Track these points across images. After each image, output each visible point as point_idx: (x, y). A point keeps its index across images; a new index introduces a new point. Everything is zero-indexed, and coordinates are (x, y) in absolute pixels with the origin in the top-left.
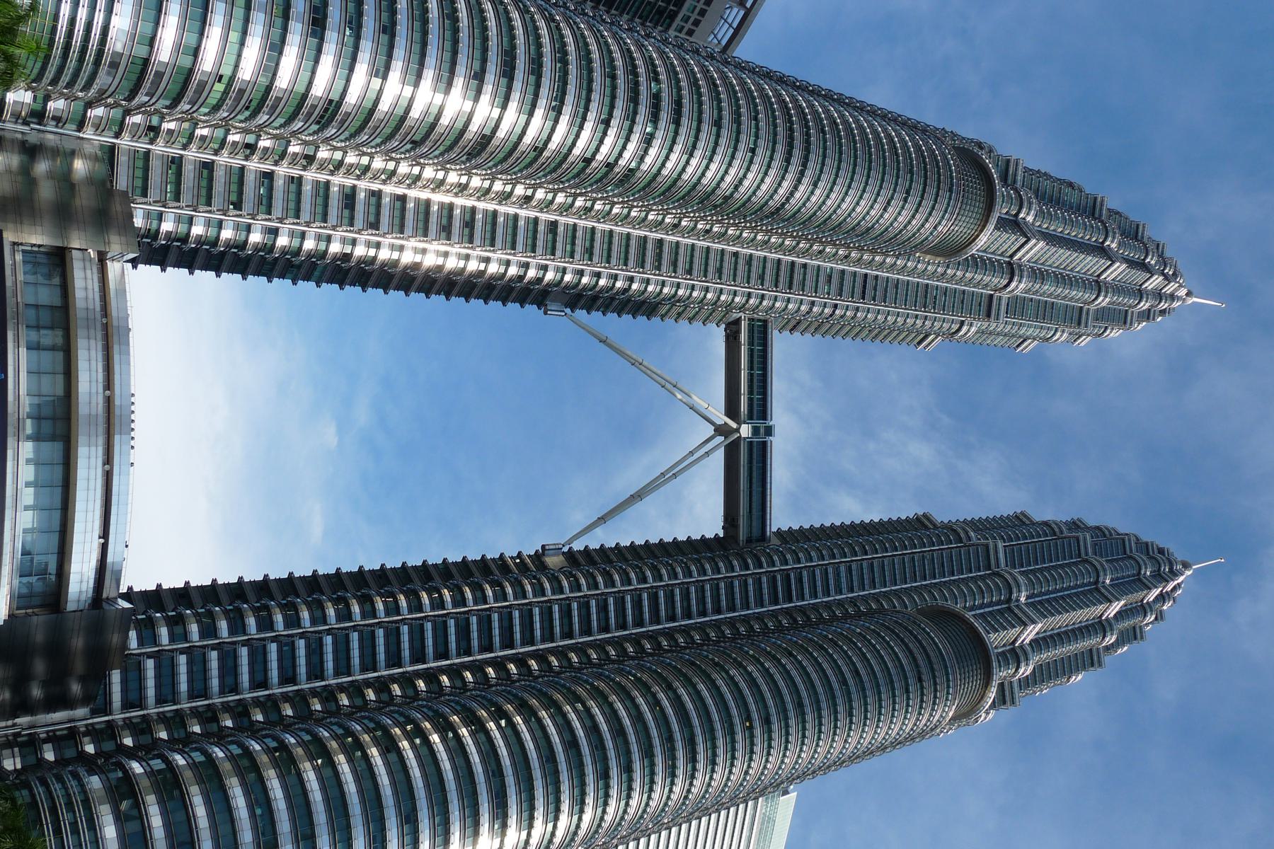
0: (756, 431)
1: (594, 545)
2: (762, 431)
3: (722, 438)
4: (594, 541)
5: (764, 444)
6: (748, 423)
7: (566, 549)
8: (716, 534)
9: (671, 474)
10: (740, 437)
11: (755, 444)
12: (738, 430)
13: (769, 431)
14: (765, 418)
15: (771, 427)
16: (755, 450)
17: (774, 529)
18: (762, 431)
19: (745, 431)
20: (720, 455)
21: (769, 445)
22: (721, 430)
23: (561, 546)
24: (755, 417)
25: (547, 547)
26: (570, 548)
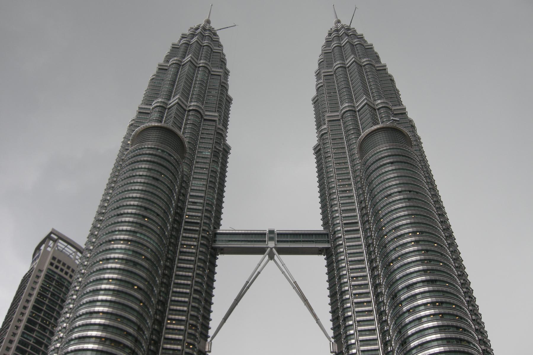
0: (271, 239)
1: (331, 325)
2: (271, 235)
3: (275, 256)
4: (328, 325)
5: (278, 234)
6: (268, 243)
7: (333, 340)
8: (325, 259)
9: (294, 284)
10: (275, 248)
11: (279, 239)
12: (271, 249)
13: (271, 232)
14: (265, 234)
15: (269, 231)
17: (322, 228)
18: (271, 235)
19: (271, 244)
20: (282, 257)
21: (278, 232)
23: (331, 343)
24: (264, 239)
25: (332, 351)
26: (332, 338)
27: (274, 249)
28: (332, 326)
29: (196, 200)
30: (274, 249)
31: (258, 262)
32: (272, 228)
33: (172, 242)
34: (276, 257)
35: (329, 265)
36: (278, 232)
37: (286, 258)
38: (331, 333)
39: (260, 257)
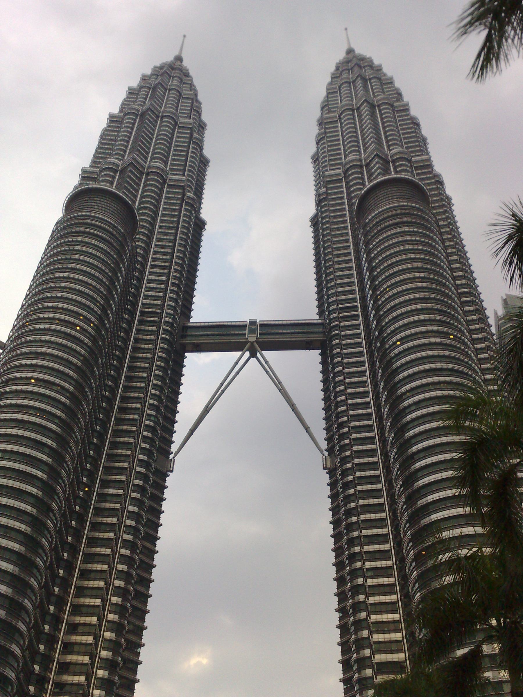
0: (253, 331)
2: (253, 327)
3: (258, 353)
5: (261, 326)
11: (261, 332)
12: (252, 343)
13: (253, 323)
14: (245, 326)
16: (264, 332)
18: (253, 327)
22: (253, 355)
24: (244, 332)
27: (255, 344)
28: (325, 436)
29: (155, 286)
30: (255, 344)
31: (235, 360)
32: (253, 318)
33: (124, 326)
34: (258, 355)
35: (324, 363)
36: (262, 323)
37: (269, 355)
38: (324, 445)
39: (237, 354)
